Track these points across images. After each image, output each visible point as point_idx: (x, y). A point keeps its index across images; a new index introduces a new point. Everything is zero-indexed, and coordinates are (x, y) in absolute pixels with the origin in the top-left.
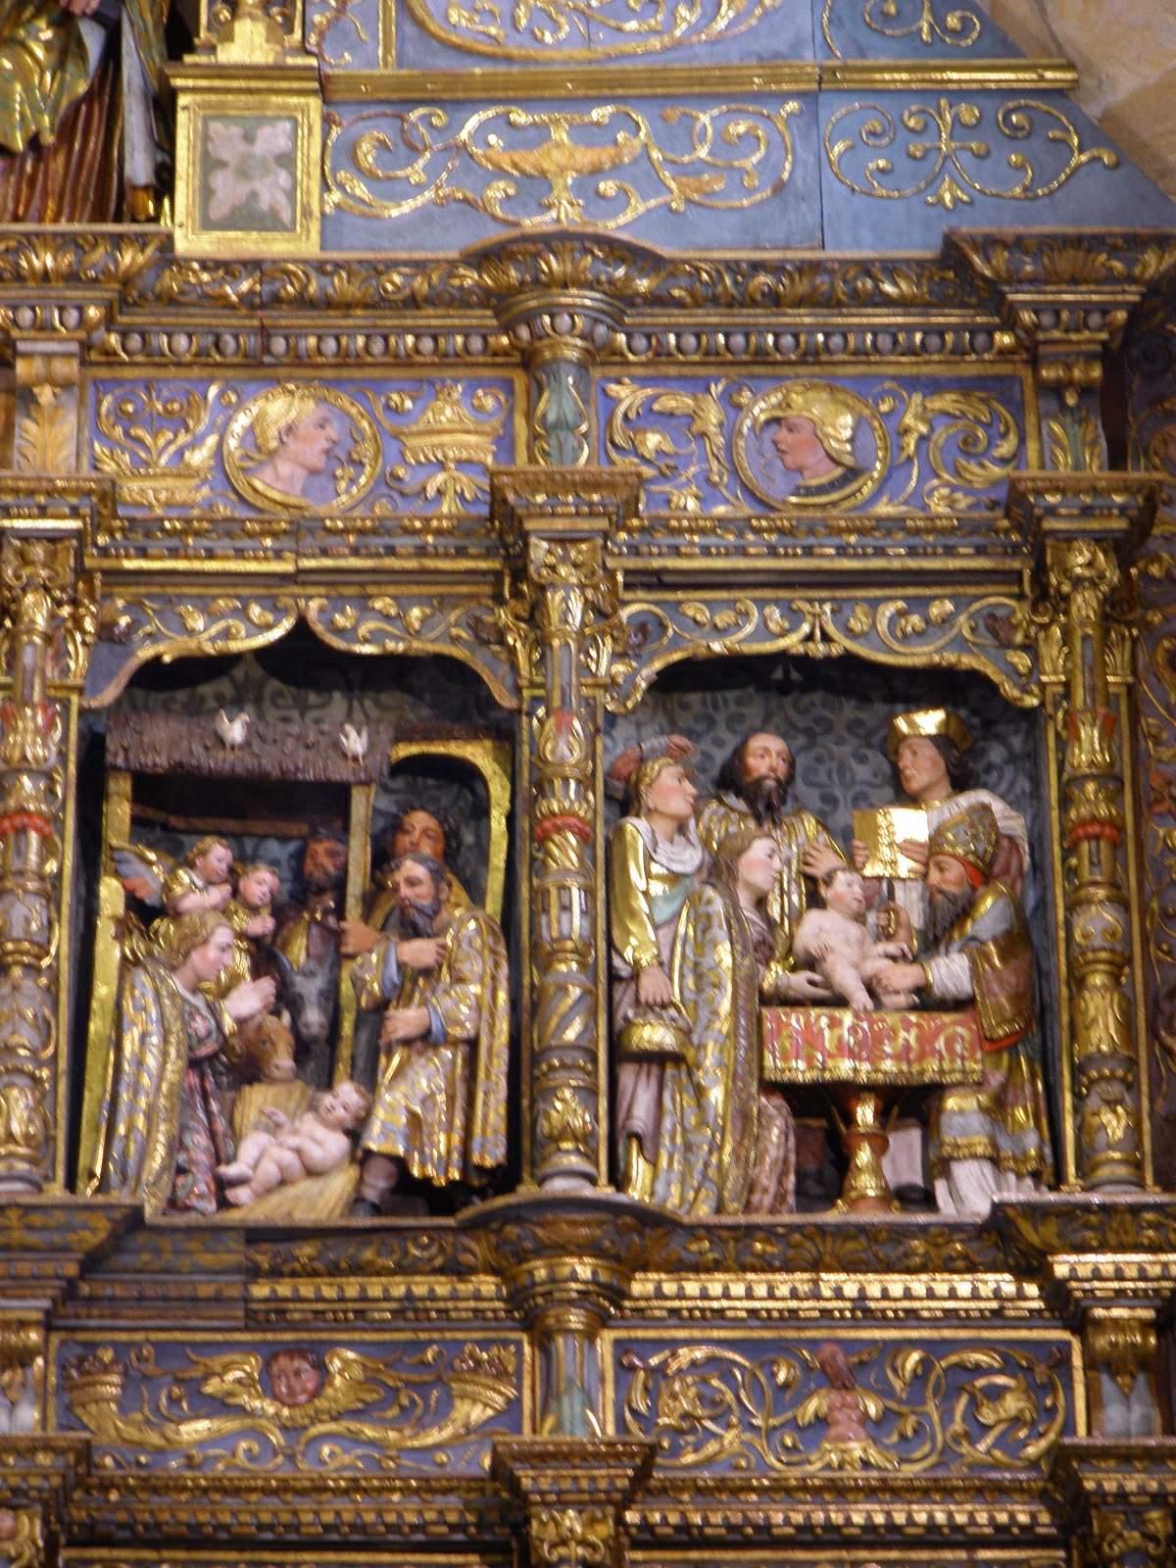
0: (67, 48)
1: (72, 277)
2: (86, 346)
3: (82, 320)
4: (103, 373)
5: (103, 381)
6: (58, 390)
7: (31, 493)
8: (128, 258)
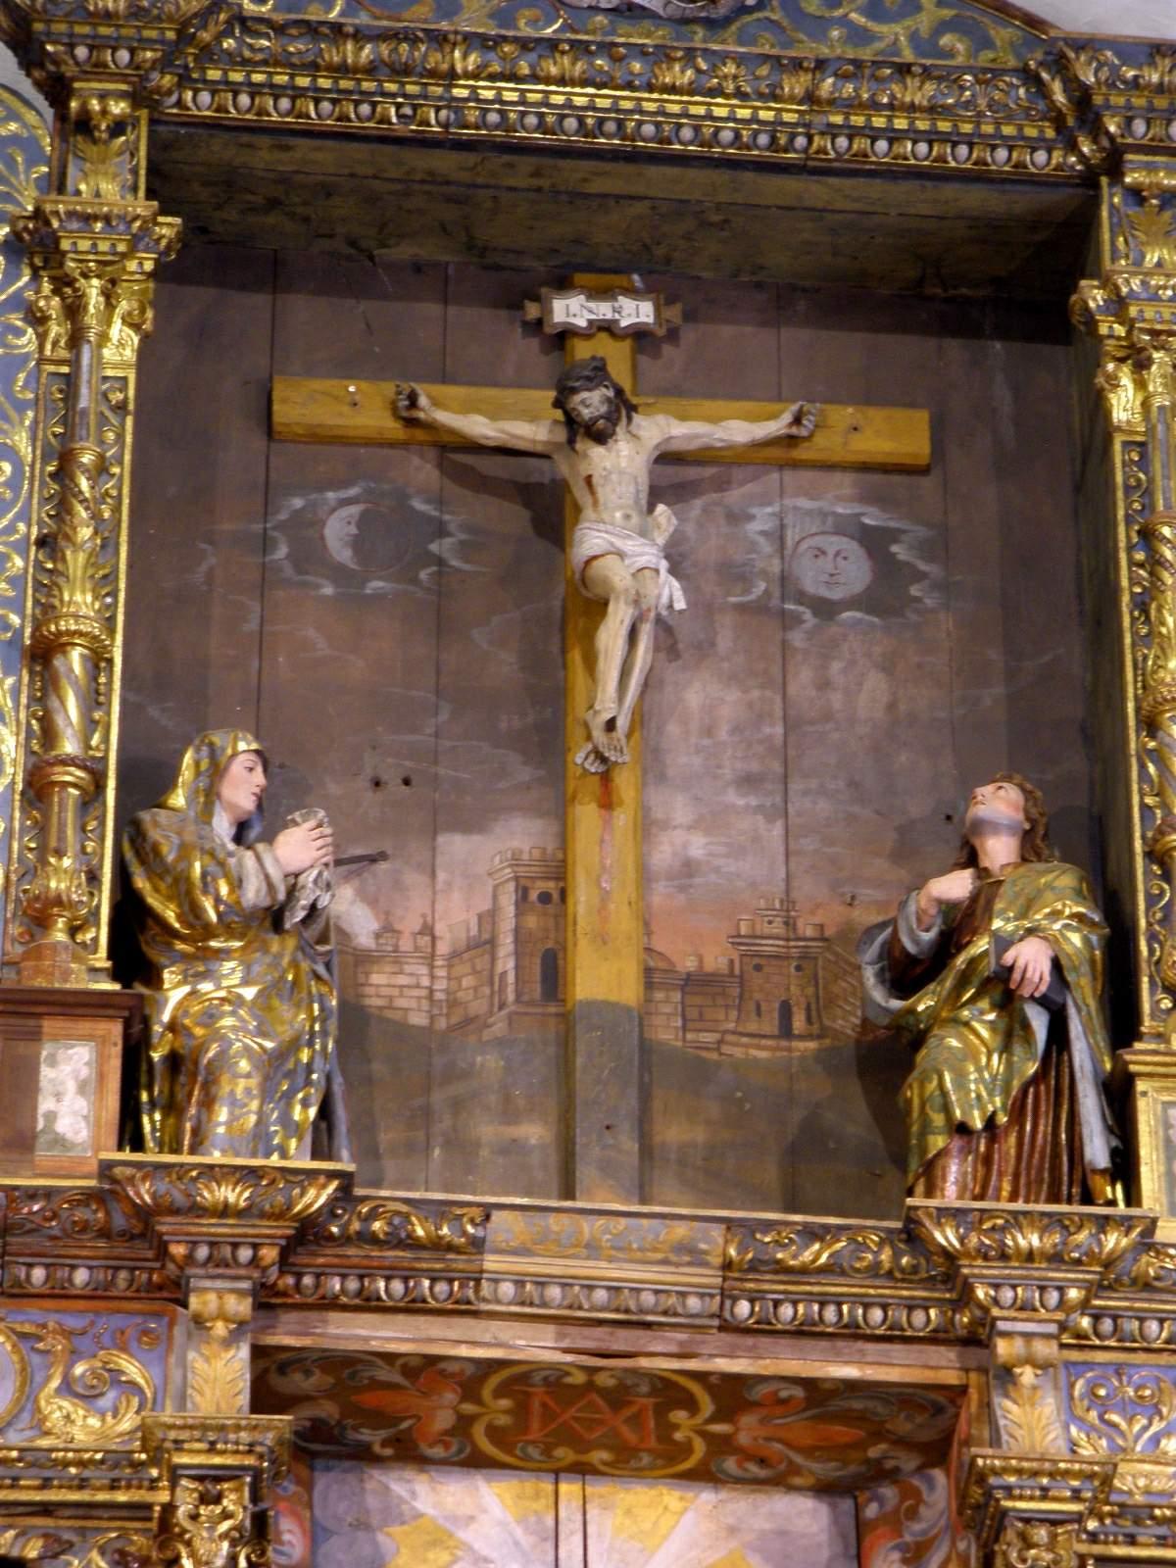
0: (1013, 1030)
1: (1056, 1258)
2: (1063, 1327)
3: (1062, 1303)
4: (1075, 1356)
5: (1075, 1364)
6: (1039, 1372)
7: (1035, 1474)
8: (1112, 1240)
